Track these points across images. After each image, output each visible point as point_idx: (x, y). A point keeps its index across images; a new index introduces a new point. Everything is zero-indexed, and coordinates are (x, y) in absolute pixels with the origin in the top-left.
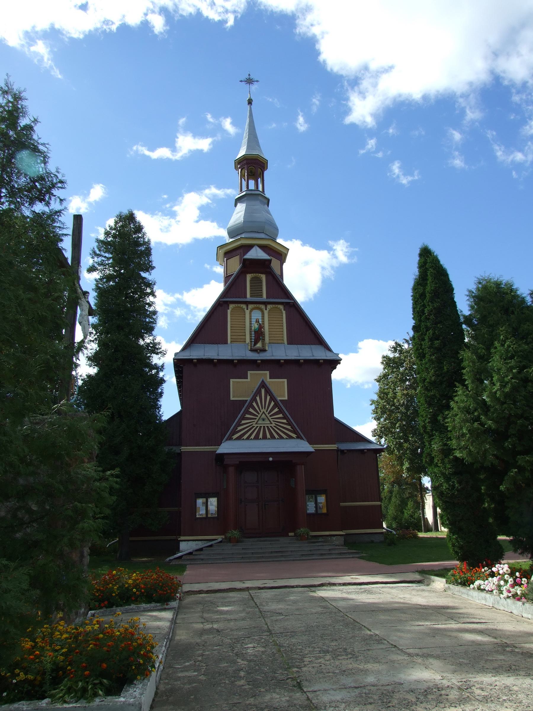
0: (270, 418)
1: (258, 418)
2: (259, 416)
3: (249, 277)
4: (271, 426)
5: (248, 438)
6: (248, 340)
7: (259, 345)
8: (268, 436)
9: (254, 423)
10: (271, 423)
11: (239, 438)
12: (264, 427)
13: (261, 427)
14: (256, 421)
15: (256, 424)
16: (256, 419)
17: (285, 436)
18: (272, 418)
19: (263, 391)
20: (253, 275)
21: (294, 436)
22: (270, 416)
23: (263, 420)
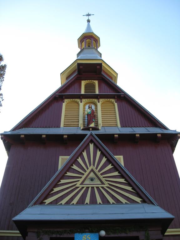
0: (101, 177)
1: (84, 177)
2: (86, 174)
3: (83, 83)
4: (102, 187)
5: (68, 203)
6: (81, 122)
7: (92, 125)
8: (99, 200)
9: (79, 183)
10: (103, 183)
11: (56, 202)
12: (93, 188)
13: (88, 188)
14: (81, 180)
15: (82, 184)
16: (81, 177)
17: (124, 201)
18: (104, 177)
19: (91, 146)
20: (87, 82)
21: (138, 200)
22: (102, 174)
23: (92, 180)
